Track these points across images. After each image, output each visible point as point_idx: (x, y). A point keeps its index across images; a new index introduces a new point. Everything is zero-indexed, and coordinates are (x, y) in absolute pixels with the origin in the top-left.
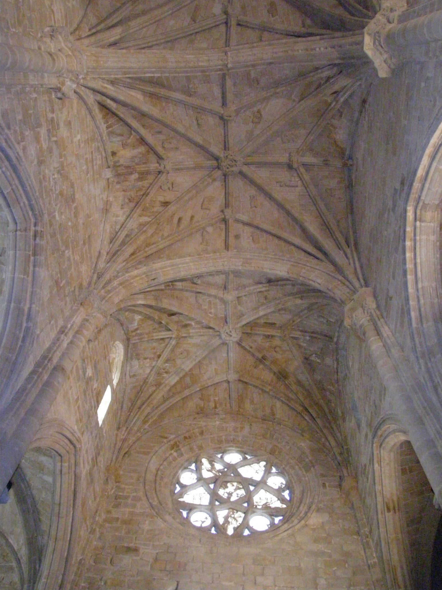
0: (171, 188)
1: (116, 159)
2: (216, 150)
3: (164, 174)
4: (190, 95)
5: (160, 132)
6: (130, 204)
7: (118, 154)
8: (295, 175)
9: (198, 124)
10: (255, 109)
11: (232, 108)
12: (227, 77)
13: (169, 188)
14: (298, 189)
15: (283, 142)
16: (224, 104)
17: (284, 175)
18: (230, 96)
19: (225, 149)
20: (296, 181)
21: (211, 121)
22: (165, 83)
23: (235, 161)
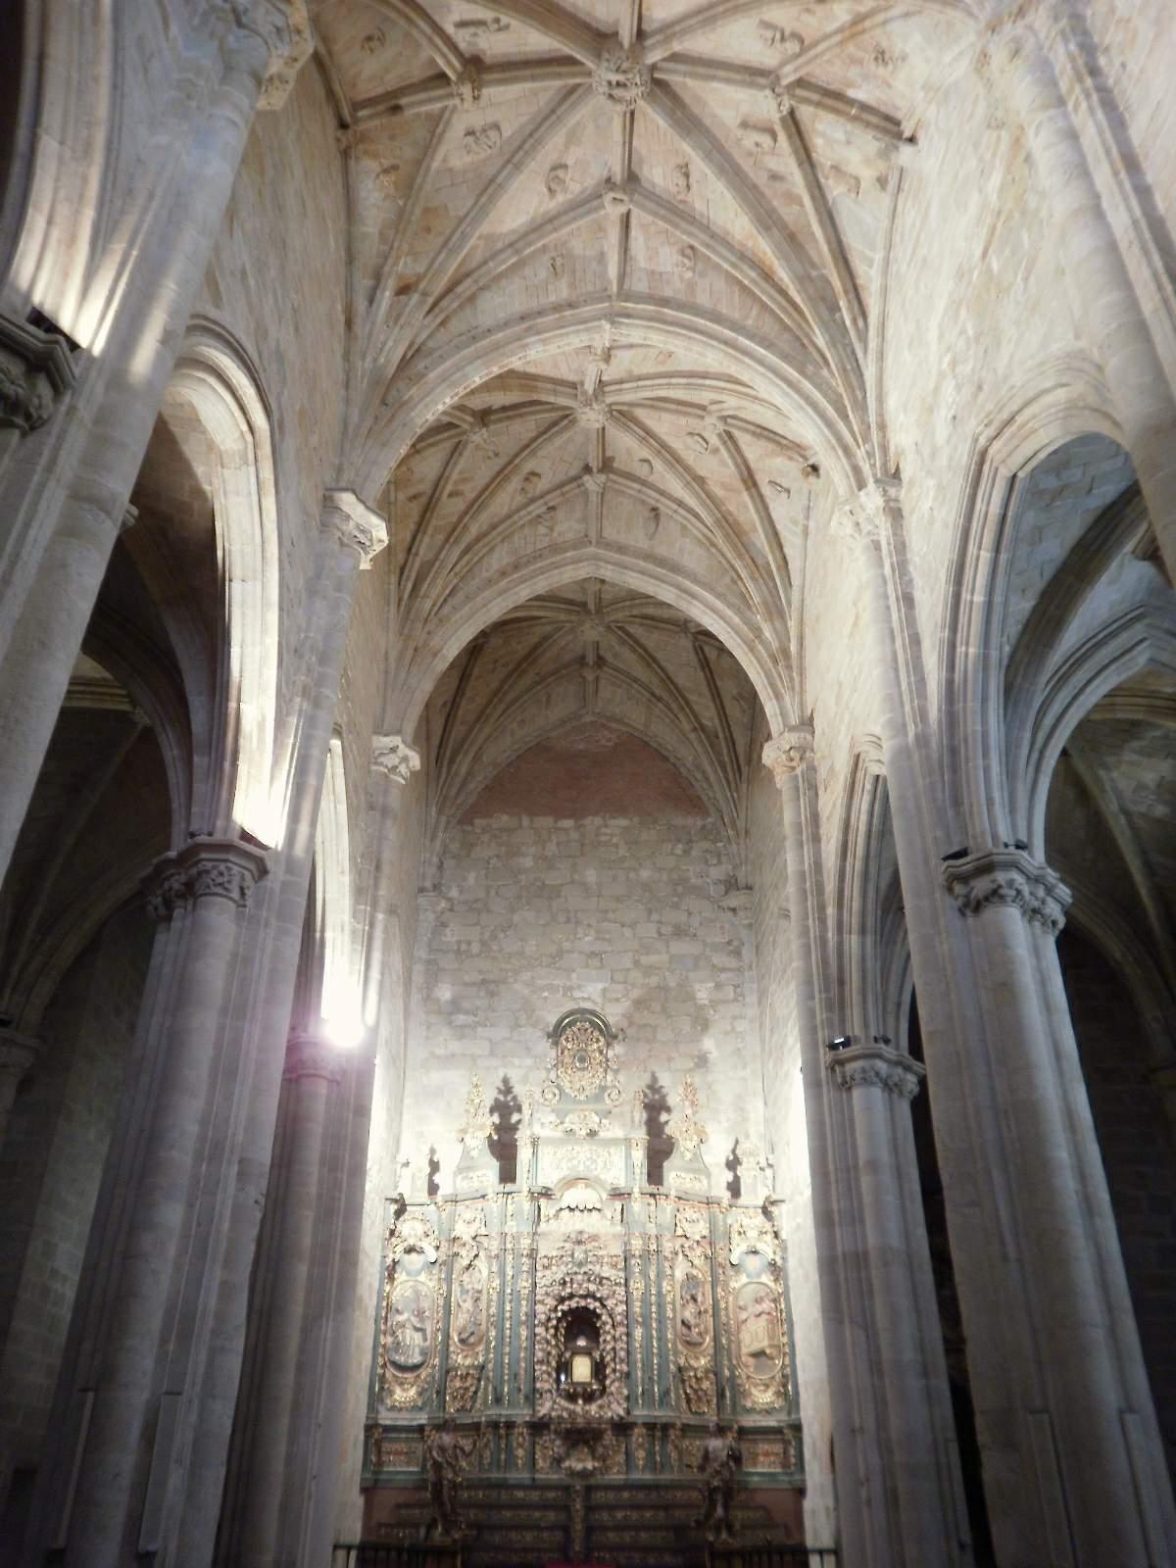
0: (778, 36)
1: (881, 165)
2: (653, 120)
3: (785, 82)
4: (692, 247)
5: (775, 177)
6: (884, 44)
7: (876, 174)
8: (462, 46)
9: (687, 175)
10: (560, 198)
11: (612, 211)
12: (615, 288)
13: (783, 39)
14: (456, 17)
15: (496, 127)
16: (626, 222)
17: (492, 45)
18: (614, 235)
19: (632, 113)
20: (462, 38)
21: (658, 175)
22: (737, 293)
23: (611, 96)
